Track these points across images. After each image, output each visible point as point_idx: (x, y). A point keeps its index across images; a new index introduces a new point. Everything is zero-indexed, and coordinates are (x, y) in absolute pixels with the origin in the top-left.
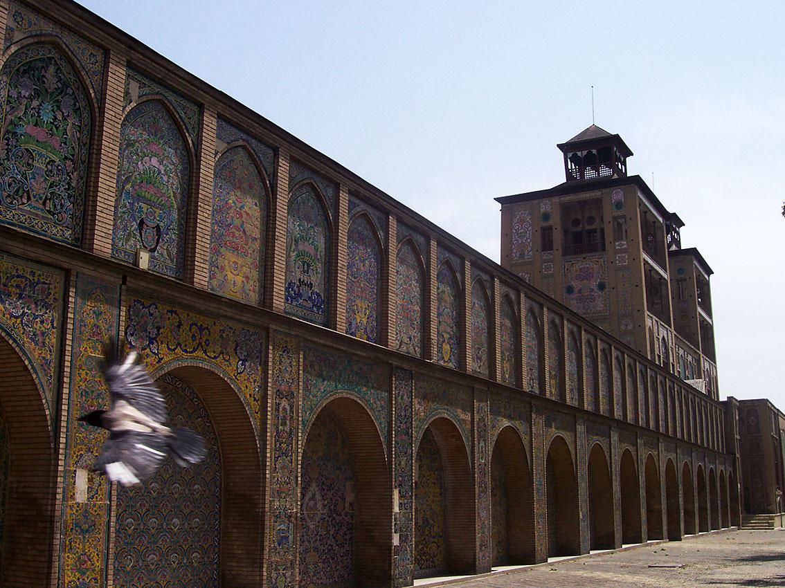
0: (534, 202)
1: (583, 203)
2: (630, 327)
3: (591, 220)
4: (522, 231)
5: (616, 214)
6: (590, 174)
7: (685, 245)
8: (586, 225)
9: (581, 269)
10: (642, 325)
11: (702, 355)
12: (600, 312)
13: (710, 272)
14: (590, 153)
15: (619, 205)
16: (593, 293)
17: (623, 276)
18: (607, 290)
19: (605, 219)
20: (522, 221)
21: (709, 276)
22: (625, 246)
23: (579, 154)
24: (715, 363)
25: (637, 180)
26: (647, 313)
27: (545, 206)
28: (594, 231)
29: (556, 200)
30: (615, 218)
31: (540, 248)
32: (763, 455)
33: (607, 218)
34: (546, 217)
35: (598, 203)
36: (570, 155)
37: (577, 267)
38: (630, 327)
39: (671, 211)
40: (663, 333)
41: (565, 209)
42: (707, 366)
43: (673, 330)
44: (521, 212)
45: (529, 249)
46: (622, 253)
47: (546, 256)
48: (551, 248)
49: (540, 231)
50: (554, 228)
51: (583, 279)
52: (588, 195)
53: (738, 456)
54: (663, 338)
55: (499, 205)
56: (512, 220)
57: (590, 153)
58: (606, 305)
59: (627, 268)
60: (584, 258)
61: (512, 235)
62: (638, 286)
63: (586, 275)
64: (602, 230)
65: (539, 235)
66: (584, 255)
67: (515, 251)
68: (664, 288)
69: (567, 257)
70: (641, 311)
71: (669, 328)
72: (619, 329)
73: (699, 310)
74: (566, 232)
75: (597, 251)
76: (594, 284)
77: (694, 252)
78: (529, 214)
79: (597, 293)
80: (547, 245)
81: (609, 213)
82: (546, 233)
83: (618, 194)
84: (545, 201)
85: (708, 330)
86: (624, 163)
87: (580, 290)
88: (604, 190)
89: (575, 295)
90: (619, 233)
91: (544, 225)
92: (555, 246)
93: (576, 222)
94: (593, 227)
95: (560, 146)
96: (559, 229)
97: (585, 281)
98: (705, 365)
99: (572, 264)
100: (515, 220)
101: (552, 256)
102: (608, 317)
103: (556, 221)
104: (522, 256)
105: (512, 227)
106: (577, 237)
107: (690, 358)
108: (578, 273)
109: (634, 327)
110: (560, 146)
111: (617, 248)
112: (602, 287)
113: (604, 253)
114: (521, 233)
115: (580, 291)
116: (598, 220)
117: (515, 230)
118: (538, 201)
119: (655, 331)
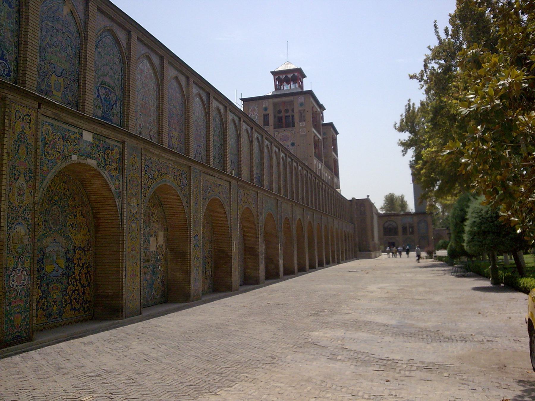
0: (260, 101)
1: (284, 103)
3: (287, 111)
6: (286, 88)
7: (326, 121)
11: (334, 175)
13: (337, 133)
14: (286, 76)
15: (302, 104)
19: (295, 111)
21: (337, 135)
23: (281, 77)
24: (339, 178)
25: (310, 93)
26: (314, 157)
27: (265, 104)
28: (288, 116)
29: (271, 100)
30: (300, 111)
33: (296, 110)
34: (266, 109)
35: (291, 103)
36: (277, 77)
39: (321, 103)
40: (320, 166)
41: (275, 105)
42: (336, 179)
43: (323, 164)
44: (253, 106)
49: (262, 116)
50: (269, 115)
51: (284, 141)
52: (287, 99)
53: (356, 225)
54: (320, 169)
57: (286, 76)
60: (285, 130)
64: (293, 116)
65: (262, 118)
66: (284, 129)
68: (320, 144)
69: (276, 130)
73: (333, 153)
74: (275, 116)
75: (290, 127)
77: (331, 125)
78: (257, 107)
80: (266, 123)
81: (297, 108)
82: (266, 117)
83: (301, 99)
84: (266, 101)
85: (336, 162)
86: (302, 82)
88: (296, 97)
90: (302, 119)
93: (280, 112)
94: (287, 114)
95: (272, 72)
96: (272, 115)
98: (335, 180)
103: (270, 112)
106: (280, 119)
107: (329, 177)
111: (301, 125)
113: (293, 128)
116: (290, 111)
119: (317, 166)
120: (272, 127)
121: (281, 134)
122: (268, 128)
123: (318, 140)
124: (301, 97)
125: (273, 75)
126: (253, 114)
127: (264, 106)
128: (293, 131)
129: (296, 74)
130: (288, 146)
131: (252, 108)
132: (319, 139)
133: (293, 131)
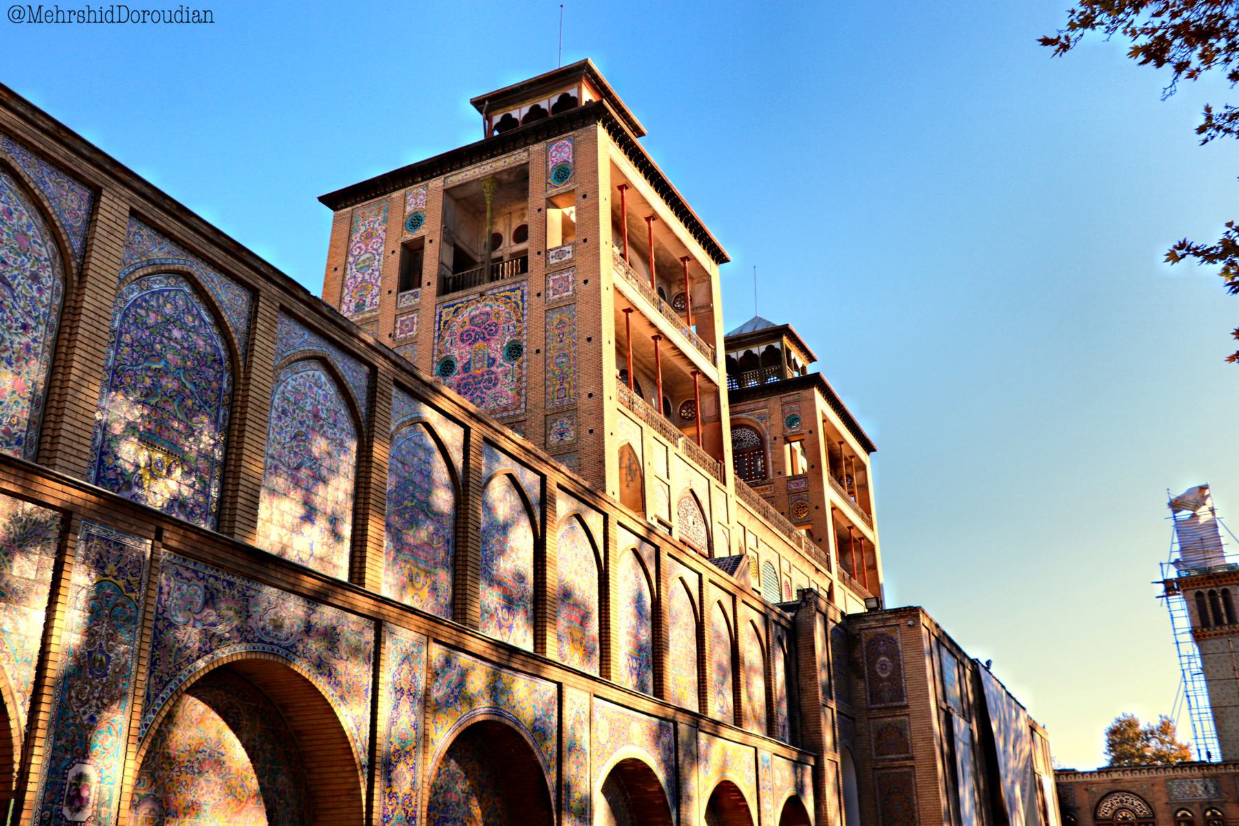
0: (396, 195)
2: (569, 437)
4: (368, 255)
5: (552, 192)
8: (513, 243)
9: (476, 316)
10: (598, 434)
11: (837, 583)
12: (506, 409)
15: (562, 173)
16: (494, 369)
17: (561, 321)
18: (525, 357)
20: (369, 236)
22: (569, 256)
29: (437, 183)
31: (395, 290)
32: (912, 758)
34: (415, 221)
35: (521, 176)
36: (497, 119)
37: (466, 314)
38: (569, 437)
44: (369, 215)
45: (376, 290)
46: (560, 271)
47: (408, 300)
48: (420, 285)
50: (427, 241)
51: (476, 340)
55: (329, 213)
56: (350, 235)
58: (519, 394)
59: (571, 303)
60: (482, 295)
61: (345, 269)
62: (594, 339)
63: (482, 331)
65: (395, 260)
66: (479, 289)
67: (347, 299)
69: (447, 297)
70: (597, 397)
71: (714, 482)
72: (545, 444)
76: (496, 348)
78: (386, 220)
79: (503, 366)
80: (410, 277)
83: (561, 150)
87: (469, 363)
88: (536, 148)
89: (455, 378)
91: (410, 236)
92: (426, 277)
95: (478, 103)
97: (480, 344)
99: (456, 311)
100: (356, 237)
101: (417, 300)
102: (521, 418)
103: (431, 230)
104: (360, 307)
105: (348, 253)
108: (467, 328)
109: (578, 433)
110: (478, 103)
111: (553, 261)
112: (514, 351)
114: (364, 261)
115: (466, 368)
117: (355, 256)
118: (403, 191)
120: (434, 288)
121: (466, 313)
122: (415, 295)
123: (694, 374)
124: (560, 143)
125: (480, 111)
126: (366, 252)
127: (409, 209)
128: (519, 292)
129: (573, 92)
130: (494, 360)
131: (363, 229)
132: (697, 371)
133: (519, 292)
